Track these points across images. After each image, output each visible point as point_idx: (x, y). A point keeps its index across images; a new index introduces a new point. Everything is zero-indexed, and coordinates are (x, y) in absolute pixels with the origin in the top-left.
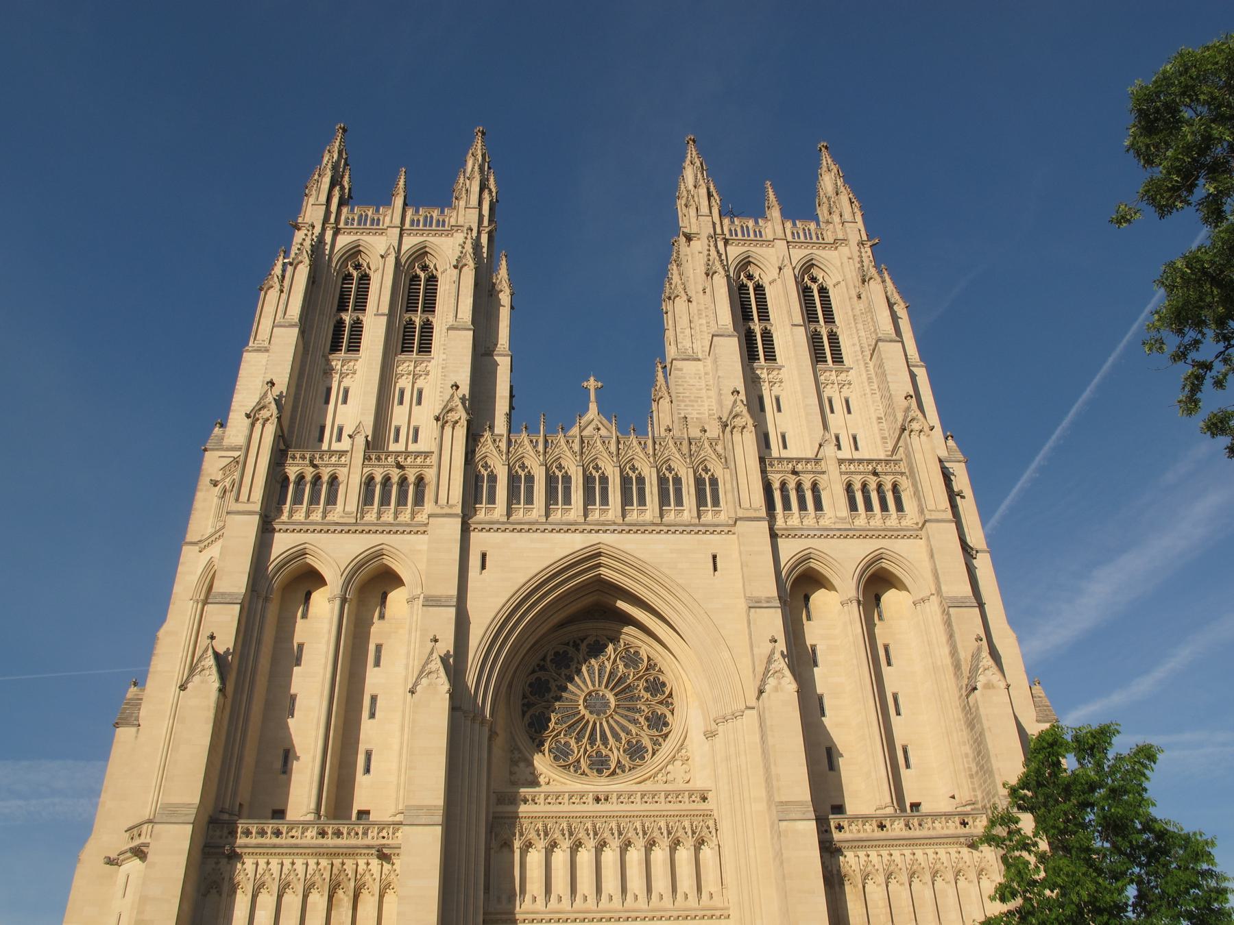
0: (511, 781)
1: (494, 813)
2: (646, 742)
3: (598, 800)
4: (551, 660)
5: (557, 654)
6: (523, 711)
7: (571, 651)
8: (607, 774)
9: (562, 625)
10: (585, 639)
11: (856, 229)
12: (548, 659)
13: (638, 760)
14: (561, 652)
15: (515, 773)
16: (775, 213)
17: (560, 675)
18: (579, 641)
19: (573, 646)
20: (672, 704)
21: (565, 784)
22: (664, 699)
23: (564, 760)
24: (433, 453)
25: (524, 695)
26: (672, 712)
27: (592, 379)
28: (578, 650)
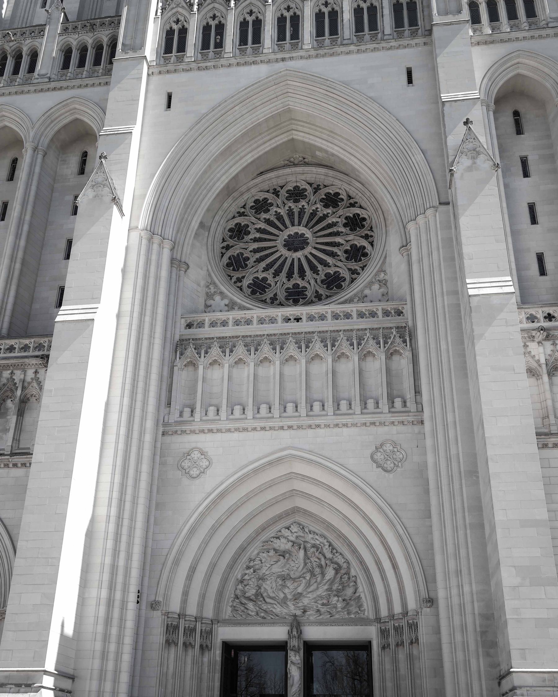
10: (284, 186)
12: (248, 207)
13: (335, 288)
15: (210, 306)
17: (259, 219)
25: (223, 239)
26: (372, 244)
28: (278, 196)
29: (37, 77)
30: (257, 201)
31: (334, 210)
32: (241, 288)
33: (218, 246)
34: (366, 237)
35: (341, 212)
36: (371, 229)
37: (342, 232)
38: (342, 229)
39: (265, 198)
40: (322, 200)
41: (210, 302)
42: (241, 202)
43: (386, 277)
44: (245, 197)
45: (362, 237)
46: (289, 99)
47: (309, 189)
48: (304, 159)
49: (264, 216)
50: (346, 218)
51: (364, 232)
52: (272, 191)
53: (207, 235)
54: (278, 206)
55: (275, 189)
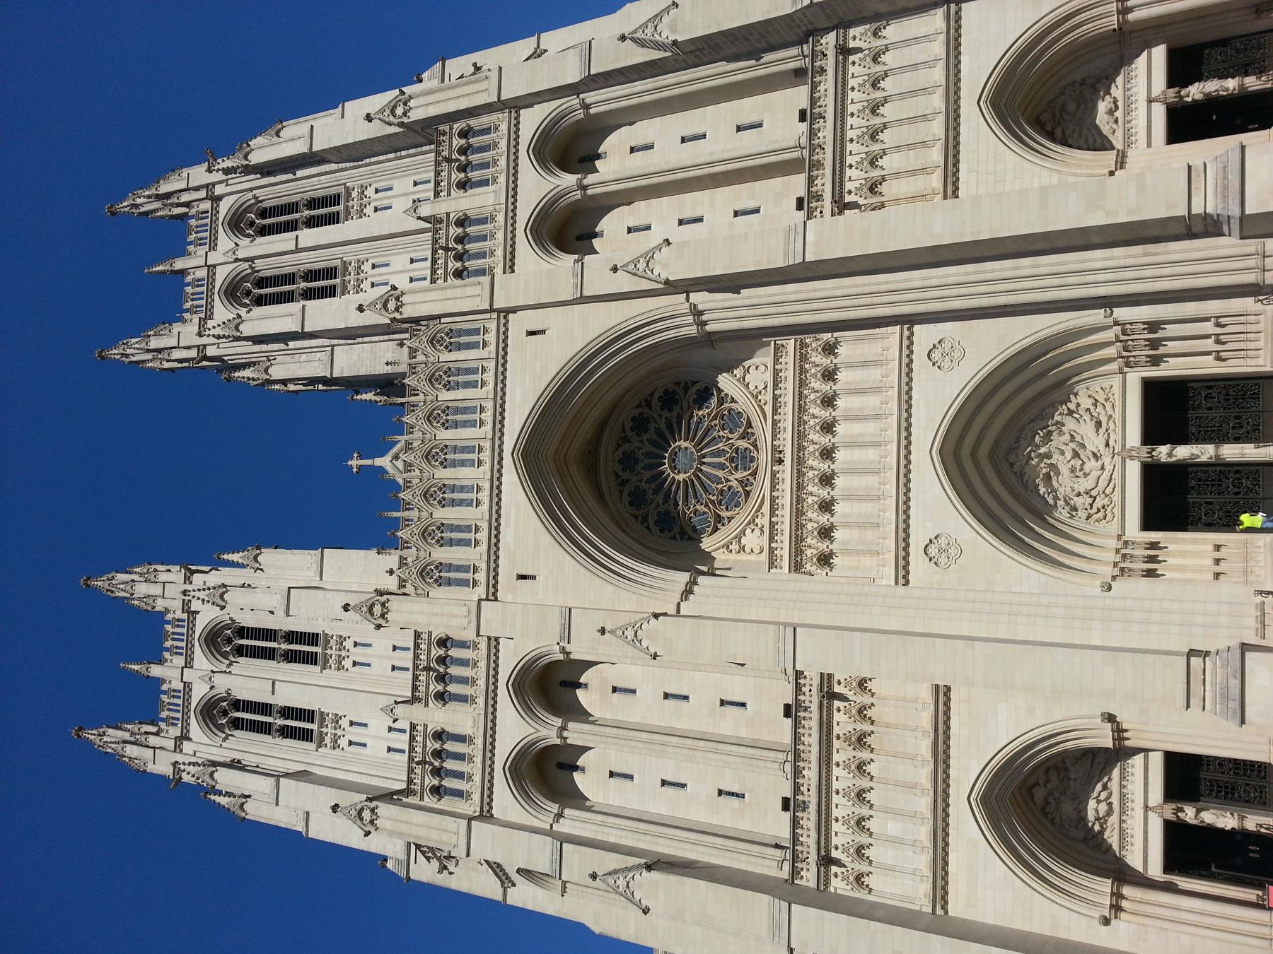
3: (781, 461)
4: (638, 509)
6: (688, 540)
8: (755, 452)
9: (601, 497)
11: (198, 174)
12: (635, 512)
16: (179, 264)
17: (653, 500)
18: (619, 480)
24: (415, 631)
27: (350, 463)
28: (628, 481)
29: (475, 730)
30: (631, 504)
31: (652, 421)
32: (730, 519)
34: (686, 388)
35: (655, 415)
36: (678, 384)
37: (678, 413)
38: (675, 414)
39: (629, 495)
40: (639, 435)
45: (686, 393)
46: (540, 454)
47: (626, 447)
48: (590, 452)
49: (650, 496)
50: (662, 409)
51: (680, 391)
52: (621, 488)
54: (641, 481)
55: (619, 485)
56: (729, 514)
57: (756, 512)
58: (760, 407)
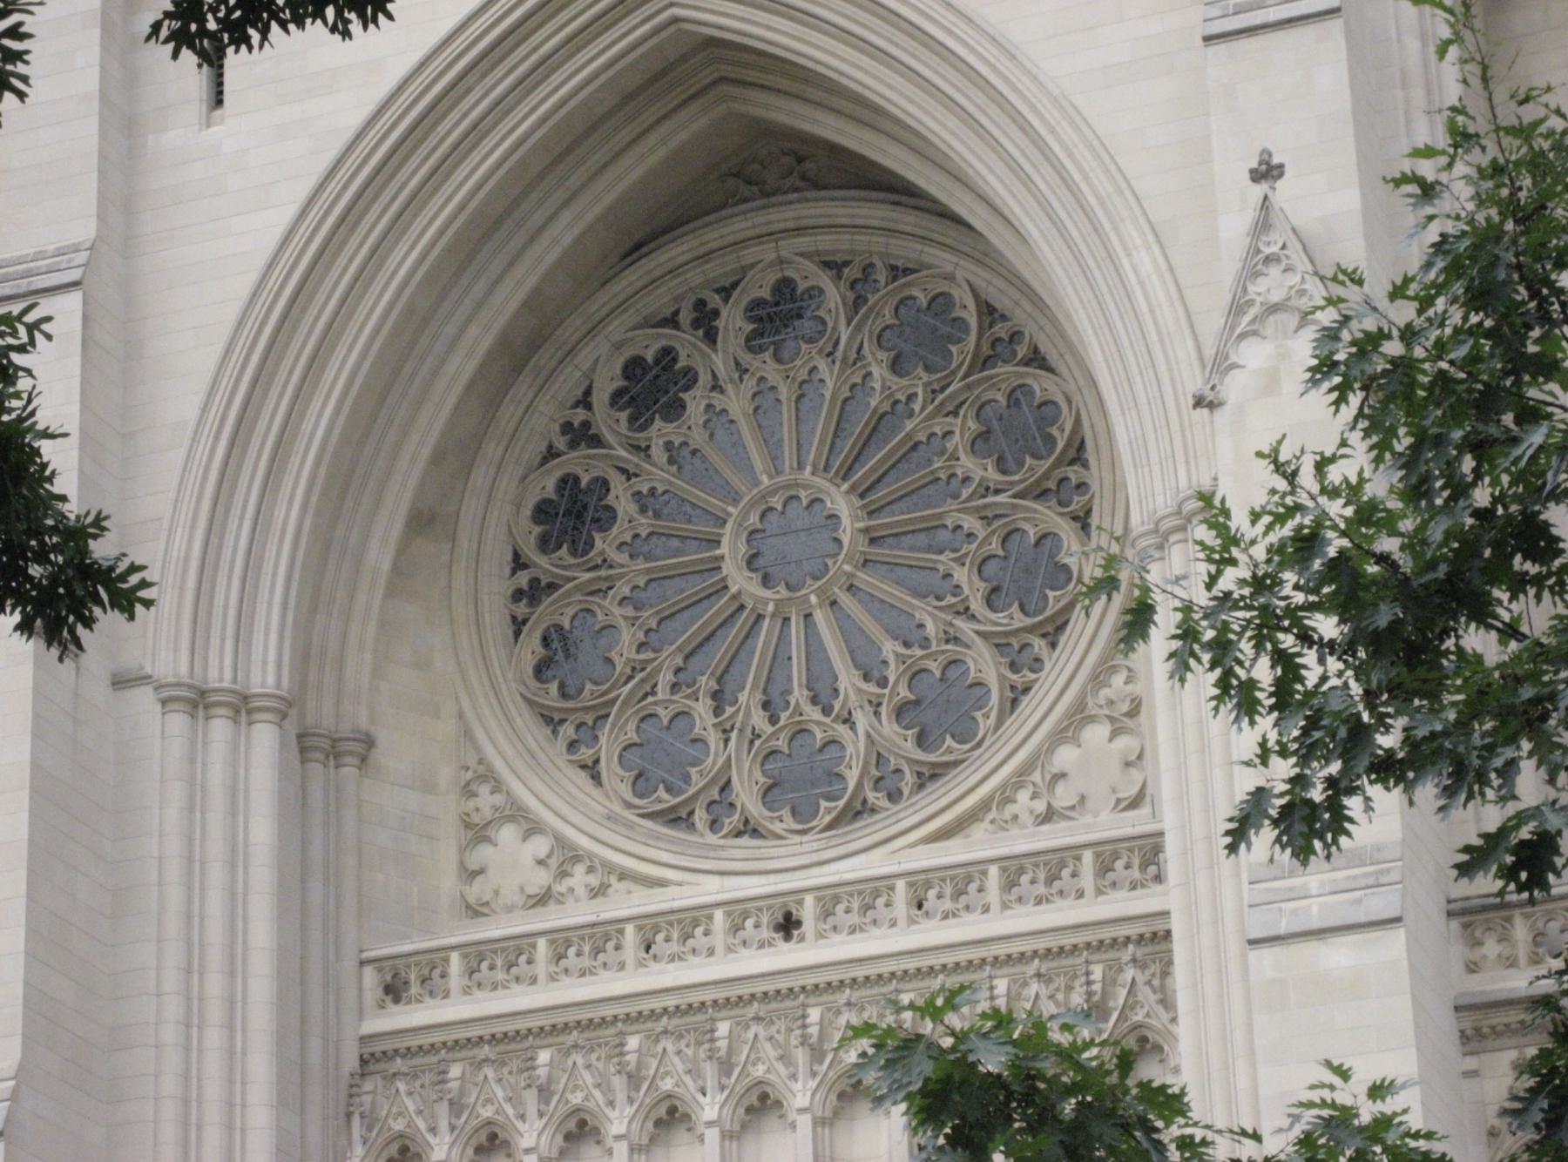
0: (468, 907)
1: (365, 1039)
2: (984, 664)
4: (616, 398)
5: (634, 368)
7: (687, 345)
10: (735, 285)
12: (601, 398)
14: (649, 356)
15: (481, 871)
18: (714, 300)
19: (696, 324)
20: (1082, 486)
21: (662, 883)
22: (1046, 476)
23: (669, 790)
25: (516, 555)
33: (497, 587)
41: (483, 853)
42: (568, 383)
43: (1136, 688)
44: (585, 358)
53: (445, 558)
56: (609, 766)
57: (609, 868)
58: (985, 806)
